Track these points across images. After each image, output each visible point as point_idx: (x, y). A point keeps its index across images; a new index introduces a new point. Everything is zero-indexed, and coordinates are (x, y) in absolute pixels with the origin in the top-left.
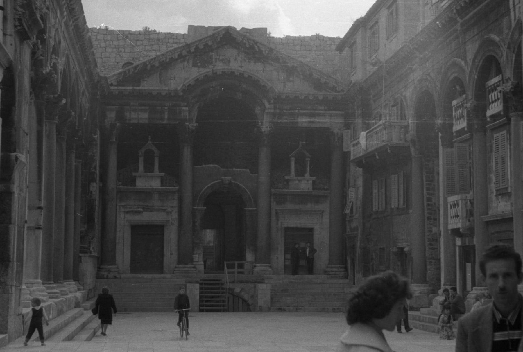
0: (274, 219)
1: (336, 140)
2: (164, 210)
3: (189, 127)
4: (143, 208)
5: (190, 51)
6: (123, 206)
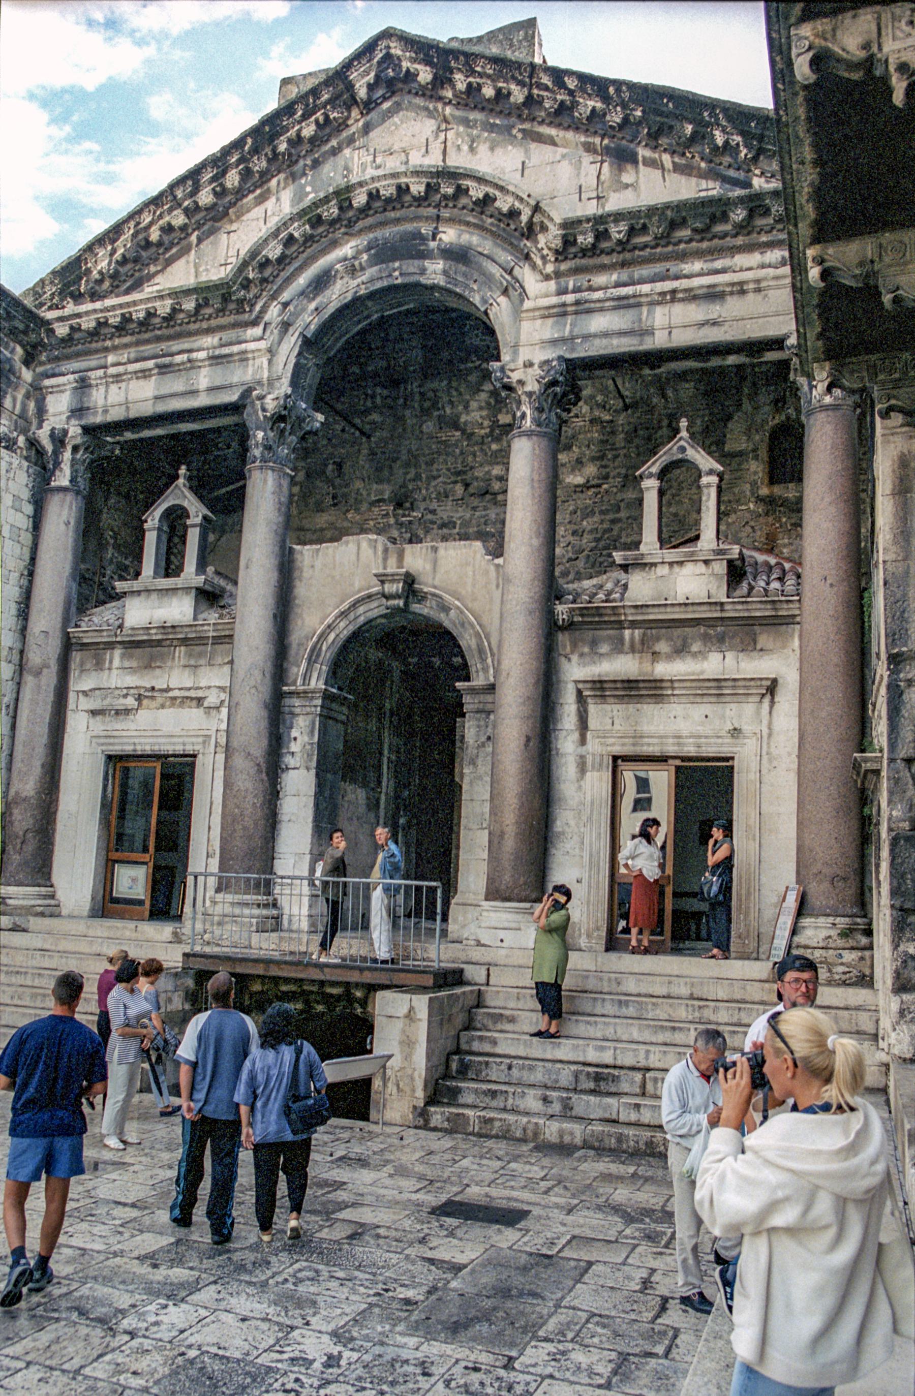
2: (200, 701)
4: (139, 698)
6: (85, 693)
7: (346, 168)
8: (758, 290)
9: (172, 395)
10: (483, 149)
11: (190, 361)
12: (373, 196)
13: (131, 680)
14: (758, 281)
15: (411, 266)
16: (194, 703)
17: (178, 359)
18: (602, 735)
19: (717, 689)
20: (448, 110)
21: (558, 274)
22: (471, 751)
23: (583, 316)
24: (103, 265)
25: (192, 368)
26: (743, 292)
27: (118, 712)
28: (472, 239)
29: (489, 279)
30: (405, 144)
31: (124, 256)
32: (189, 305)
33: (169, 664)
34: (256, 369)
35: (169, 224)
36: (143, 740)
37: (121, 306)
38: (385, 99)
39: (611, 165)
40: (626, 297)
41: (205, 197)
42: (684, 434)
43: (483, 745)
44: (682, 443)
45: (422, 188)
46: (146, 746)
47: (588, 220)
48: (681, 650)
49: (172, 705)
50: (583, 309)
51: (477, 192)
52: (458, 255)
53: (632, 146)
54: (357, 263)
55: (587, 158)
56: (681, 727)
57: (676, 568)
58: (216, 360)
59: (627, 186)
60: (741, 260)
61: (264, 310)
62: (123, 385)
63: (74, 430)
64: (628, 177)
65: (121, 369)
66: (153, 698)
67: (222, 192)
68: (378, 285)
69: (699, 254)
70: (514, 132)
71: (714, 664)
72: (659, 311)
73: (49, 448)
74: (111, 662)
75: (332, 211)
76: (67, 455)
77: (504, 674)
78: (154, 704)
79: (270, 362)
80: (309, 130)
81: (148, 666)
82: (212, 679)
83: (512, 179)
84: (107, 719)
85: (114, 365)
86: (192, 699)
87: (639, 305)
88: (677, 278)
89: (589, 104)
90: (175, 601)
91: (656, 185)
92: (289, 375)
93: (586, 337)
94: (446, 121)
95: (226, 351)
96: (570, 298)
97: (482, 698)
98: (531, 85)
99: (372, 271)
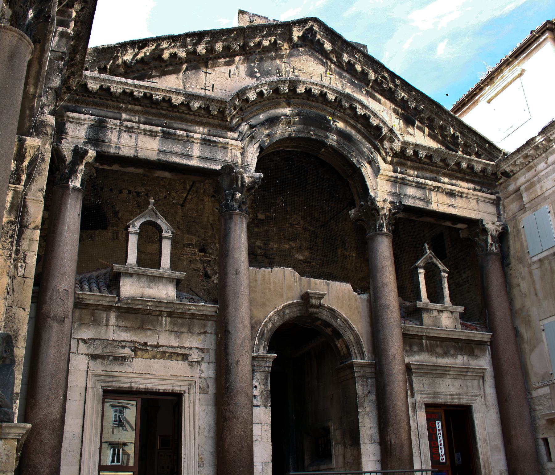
1: (490, 241)
2: (185, 357)
3: (243, 178)
4: (135, 350)
6: (85, 341)
7: (278, 69)
8: (467, 198)
11: (188, 136)
12: (308, 91)
13: (124, 336)
14: (467, 194)
15: (321, 133)
16: (180, 358)
17: (180, 132)
18: (421, 393)
19: (463, 373)
20: (333, 66)
21: (391, 163)
22: (360, 400)
23: (404, 186)
24: (128, 57)
25: (188, 141)
26: (462, 197)
27: (116, 358)
29: (362, 153)
30: (311, 72)
31: (142, 58)
32: (196, 105)
33: (158, 328)
34: (233, 155)
35: (175, 54)
36: (138, 380)
37: (146, 87)
38: (301, 46)
39: (403, 121)
40: (421, 183)
41: (201, 49)
42: (428, 251)
43: (366, 396)
44: (430, 255)
45: (334, 98)
46: (142, 384)
47: (413, 144)
48: (445, 354)
49: (162, 357)
50: (404, 183)
51: (360, 111)
53: (413, 118)
54: (293, 120)
55: (394, 116)
57: (441, 314)
58: (205, 142)
59: (411, 134)
60: (460, 183)
61: (239, 125)
62: (134, 136)
63: (92, 153)
64: (410, 130)
65: (134, 125)
66: (146, 351)
67: (210, 50)
68: (302, 135)
69: (445, 175)
70: (363, 89)
71: (460, 360)
72: (433, 194)
74: (108, 320)
75: (285, 89)
76: (82, 167)
77: (391, 357)
78: (146, 355)
79: (242, 154)
80: (266, 43)
81: (141, 328)
84: (107, 362)
85: (125, 120)
86: (178, 354)
87: (425, 189)
88: (439, 181)
89: (402, 94)
90: (161, 287)
91: (420, 138)
92: (255, 165)
93: (406, 196)
94: (331, 70)
95: (215, 139)
96: (400, 176)
97: (364, 369)
98: (380, 74)
99: (301, 126)
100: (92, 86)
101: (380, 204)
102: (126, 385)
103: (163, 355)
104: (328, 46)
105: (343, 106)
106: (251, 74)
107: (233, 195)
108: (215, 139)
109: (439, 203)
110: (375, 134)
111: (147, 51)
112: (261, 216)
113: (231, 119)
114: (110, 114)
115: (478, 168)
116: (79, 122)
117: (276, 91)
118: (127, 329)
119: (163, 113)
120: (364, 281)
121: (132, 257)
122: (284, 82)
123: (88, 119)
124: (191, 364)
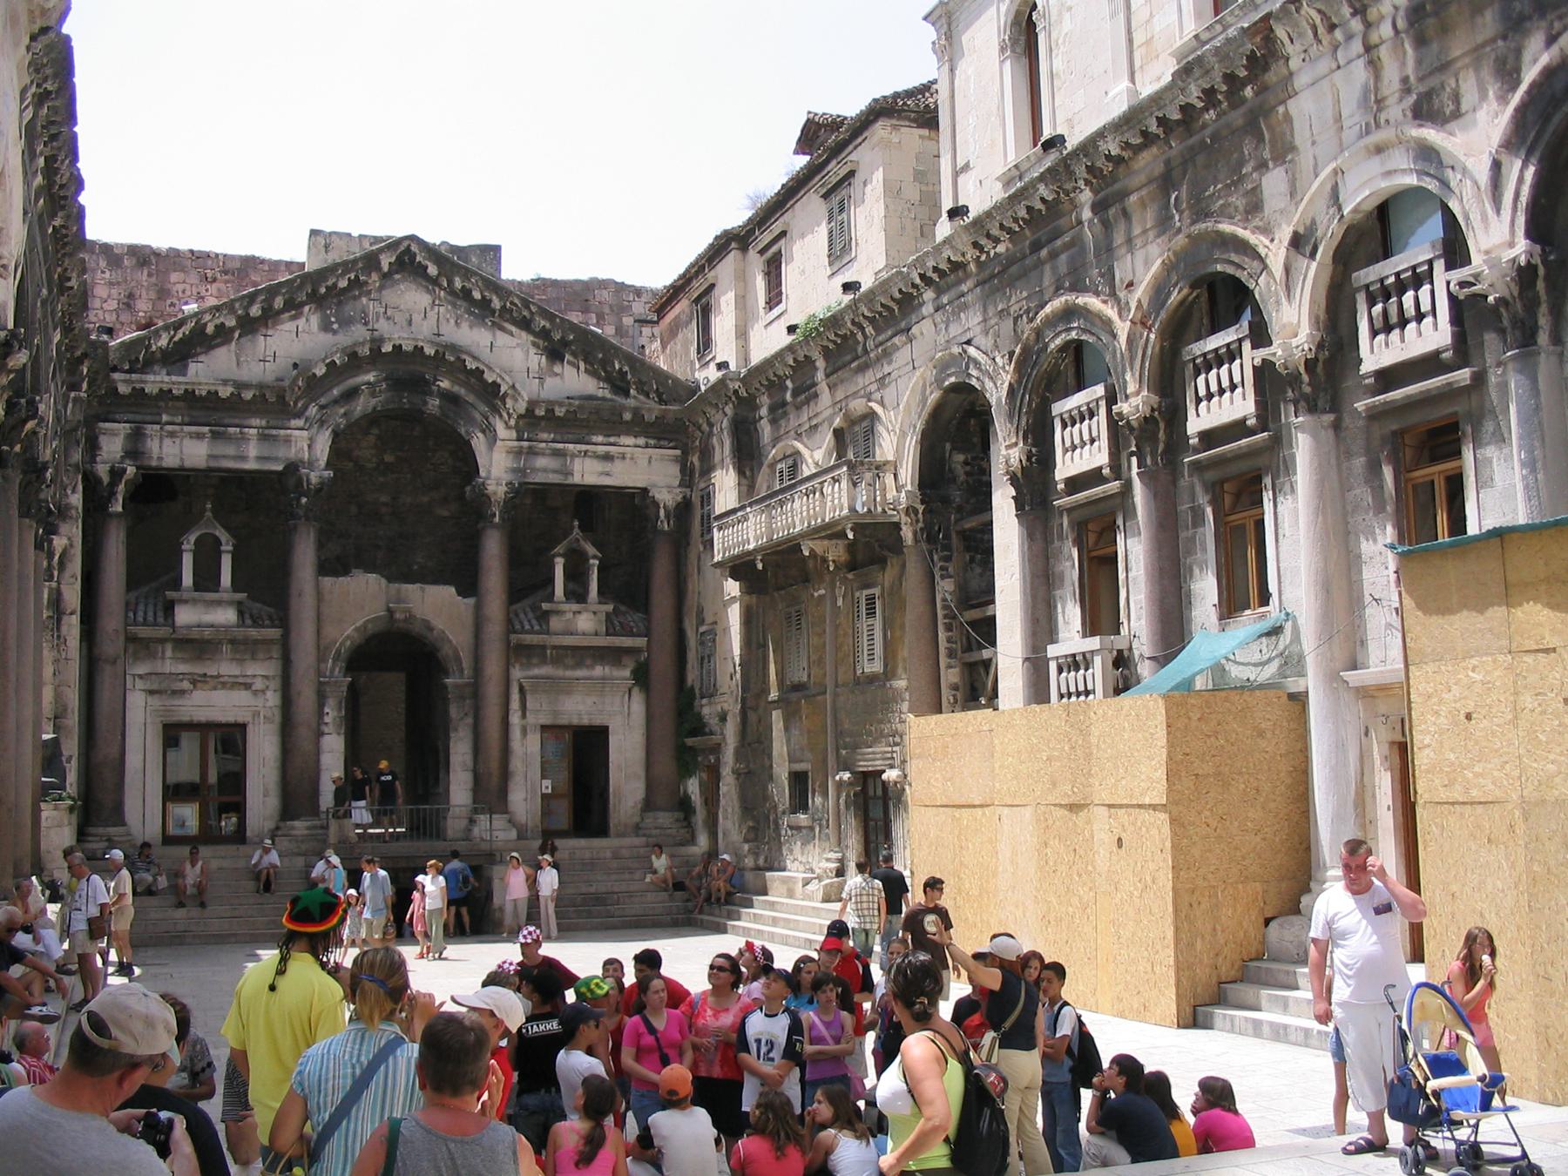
0: (515, 704)
2: (247, 686)
4: (194, 683)
5: (315, 292)
6: (141, 677)
9: (224, 457)
10: (465, 326)
12: (397, 348)
13: (183, 668)
17: (232, 430)
24: (163, 342)
27: (174, 692)
28: (461, 391)
29: (471, 421)
32: (248, 395)
41: (255, 311)
42: (576, 530)
46: (202, 716)
48: (579, 665)
50: (532, 452)
51: (471, 365)
52: (450, 398)
55: (533, 351)
56: (579, 708)
61: (306, 408)
62: (178, 441)
63: (131, 470)
64: (557, 369)
72: (577, 461)
73: (106, 479)
75: (365, 351)
76: (121, 487)
79: (309, 446)
80: (343, 284)
82: (262, 670)
83: (485, 354)
93: (534, 470)
96: (525, 444)
100: (123, 389)
101: (491, 488)
102: (186, 719)
103: (224, 685)
104: (432, 270)
105: (450, 359)
106: (326, 327)
107: (298, 500)
108: (274, 432)
109: (587, 472)
110: (492, 394)
111: (186, 329)
112: (389, 458)
113: (295, 404)
114: (148, 418)
115: (650, 417)
116: (114, 434)
117: (353, 355)
118: (184, 660)
119: (209, 410)
120: (468, 585)
121: (188, 579)
122: (363, 344)
123: (123, 429)
124: (255, 693)
